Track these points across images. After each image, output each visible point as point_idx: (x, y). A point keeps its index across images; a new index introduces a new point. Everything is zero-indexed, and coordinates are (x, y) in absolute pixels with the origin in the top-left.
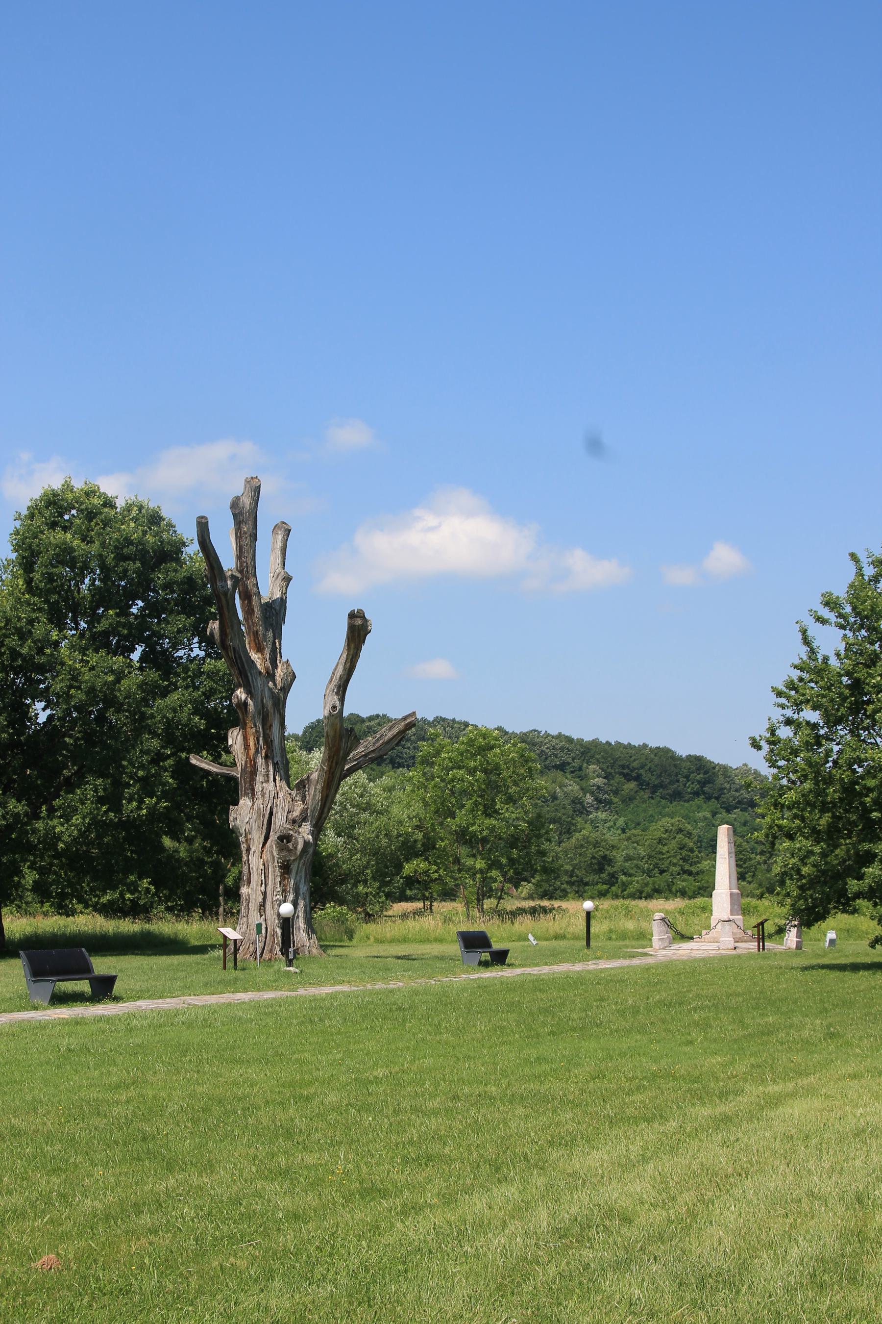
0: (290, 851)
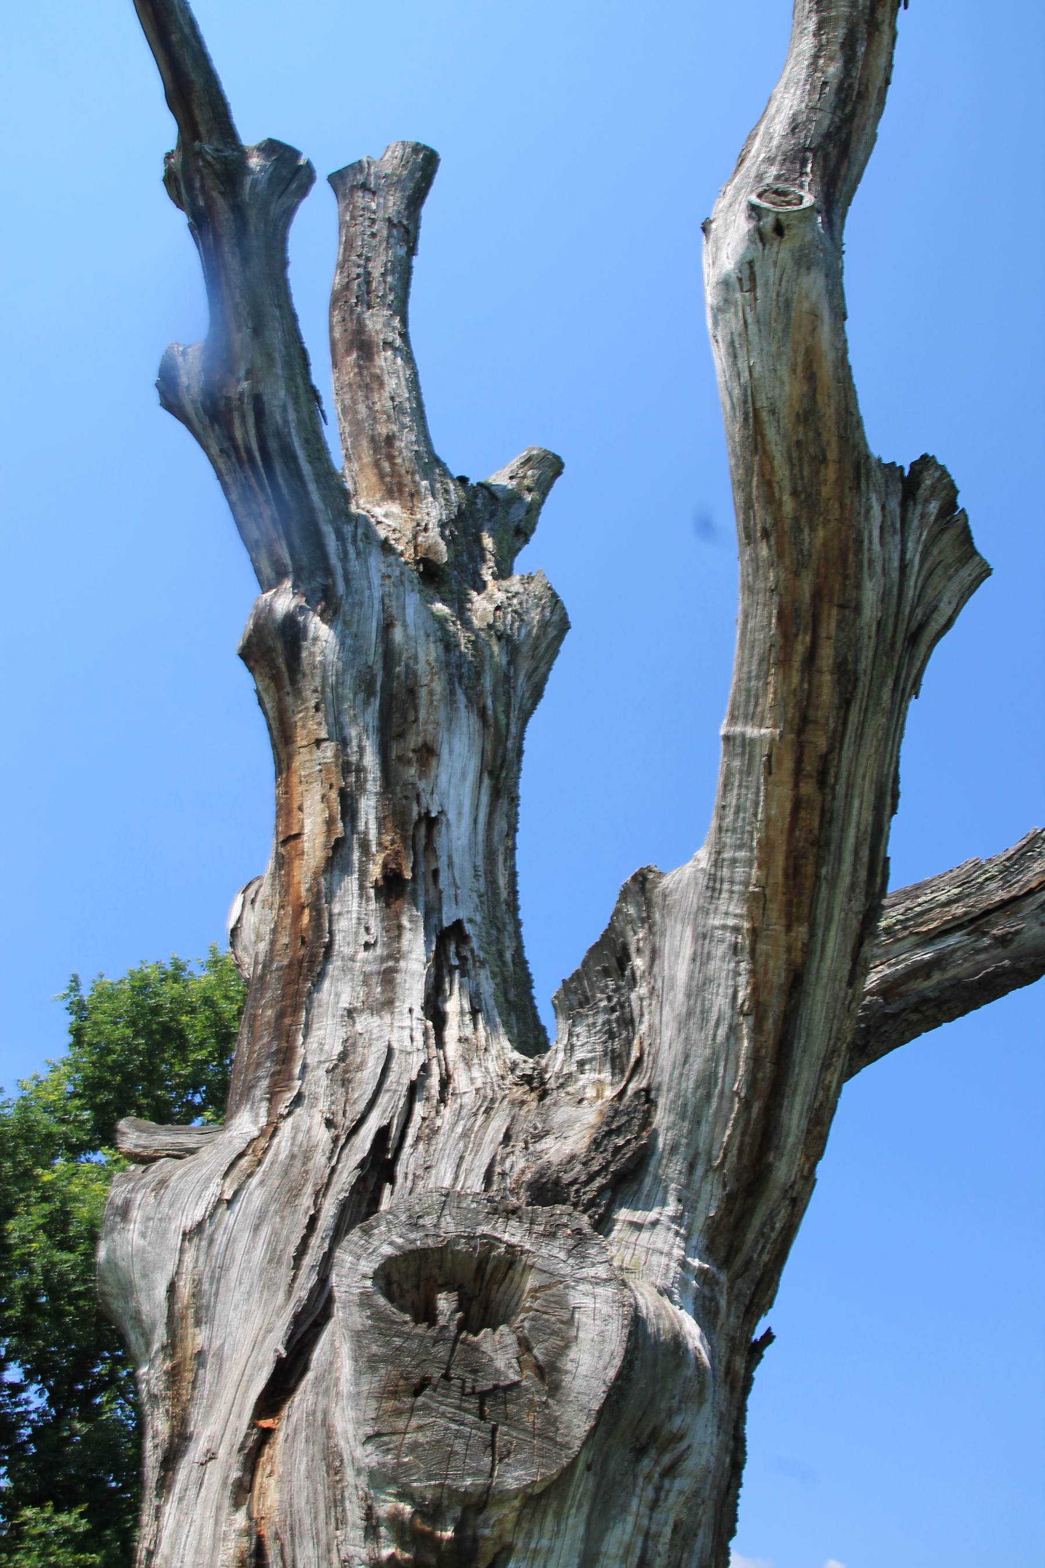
0: (491, 1400)
